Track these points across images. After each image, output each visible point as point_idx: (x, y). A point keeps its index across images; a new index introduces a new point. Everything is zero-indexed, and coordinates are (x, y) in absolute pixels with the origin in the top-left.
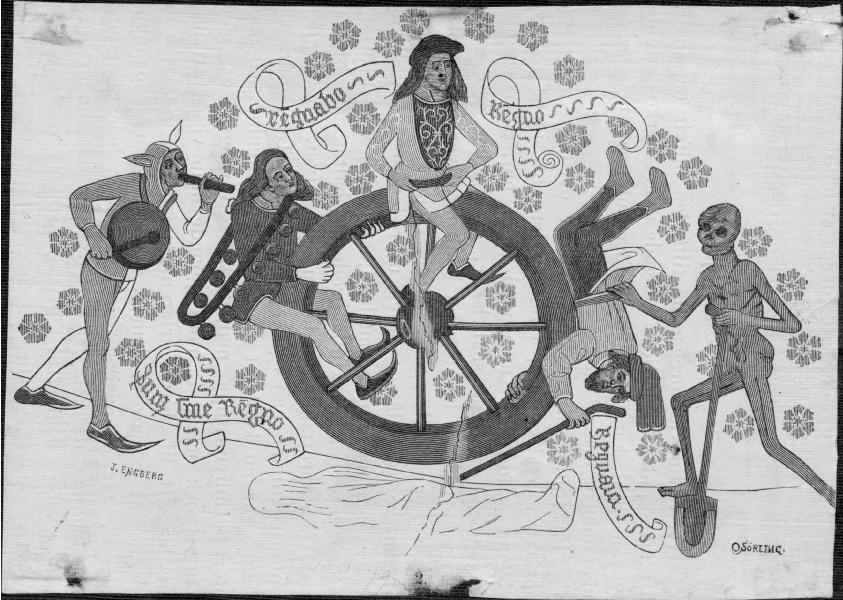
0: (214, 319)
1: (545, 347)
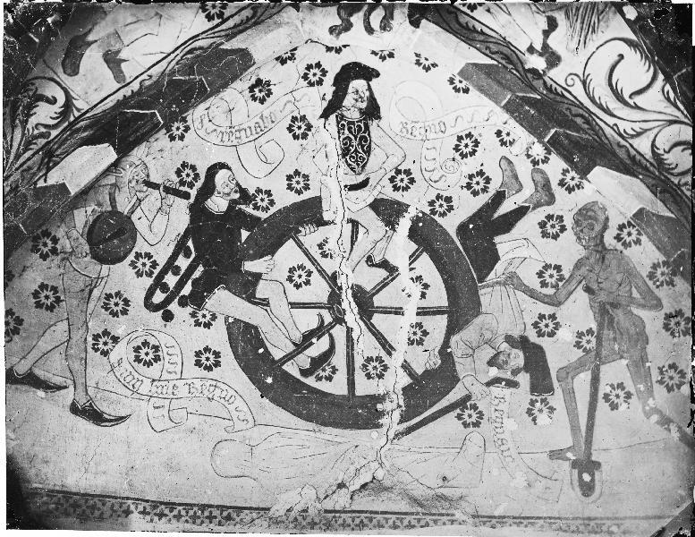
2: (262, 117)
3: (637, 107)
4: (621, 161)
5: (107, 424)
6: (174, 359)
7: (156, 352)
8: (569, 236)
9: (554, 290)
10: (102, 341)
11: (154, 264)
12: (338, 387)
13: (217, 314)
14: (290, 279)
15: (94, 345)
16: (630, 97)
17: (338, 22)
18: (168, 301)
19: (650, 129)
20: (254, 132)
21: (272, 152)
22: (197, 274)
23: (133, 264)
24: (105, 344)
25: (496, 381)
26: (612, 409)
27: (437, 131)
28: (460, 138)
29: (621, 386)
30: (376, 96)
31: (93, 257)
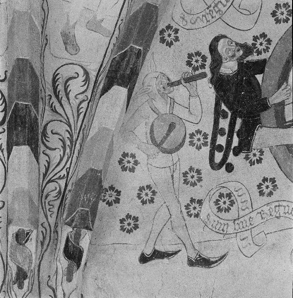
0: (231, 158)
5: (215, 264)
6: (244, 198)
7: (229, 198)
15: (188, 212)
18: (225, 157)
22: (237, 127)
23: (192, 144)
24: (195, 208)
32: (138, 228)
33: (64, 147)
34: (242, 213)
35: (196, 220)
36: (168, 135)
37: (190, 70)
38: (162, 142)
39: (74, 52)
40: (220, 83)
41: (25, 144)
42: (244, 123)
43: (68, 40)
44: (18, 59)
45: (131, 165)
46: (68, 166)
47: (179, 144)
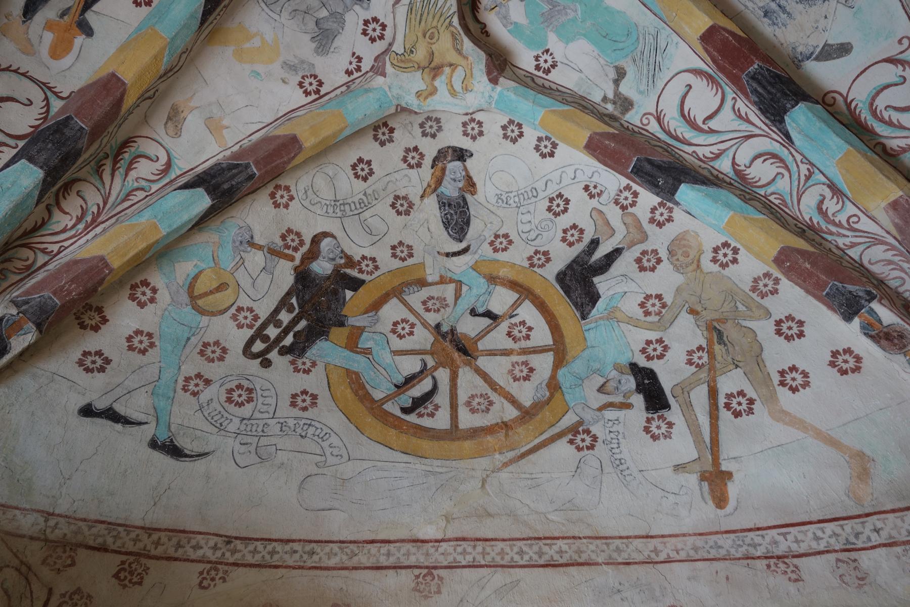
0: (273, 355)
1: (559, 363)
2: (365, 194)
3: (712, 131)
4: (705, 177)
5: (187, 459)
6: (268, 401)
8: (665, 267)
9: (657, 318)
10: (192, 383)
11: (256, 318)
12: (441, 421)
13: (318, 362)
14: (394, 331)
15: (184, 386)
16: (704, 123)
17: (423, 87)
18: (267, 350)
19: (727, 149)
20: (358, 206)
21: (374, 222)
23: (234, 317)
24: (197, 385)
25: (611, 405)
26: (736, 417)
27: (530, 195)
28: (551, 200)
29: (741, 393)
30: (472, 174)
31: (193, 308)
32: (104, 372)
33: (79, 220)
34: (257, 415)
35: (193, 400)
36: (211, 292)
37: (280, 243)
38: (201, 296)
39: (171, 132)
40: (303, 277)
41: (41, 168)
42: (309, 328)
43: (175, 118)
44: (113, 75)
45: (143, 298)
46: (66, 244)
47: (220, 309)
